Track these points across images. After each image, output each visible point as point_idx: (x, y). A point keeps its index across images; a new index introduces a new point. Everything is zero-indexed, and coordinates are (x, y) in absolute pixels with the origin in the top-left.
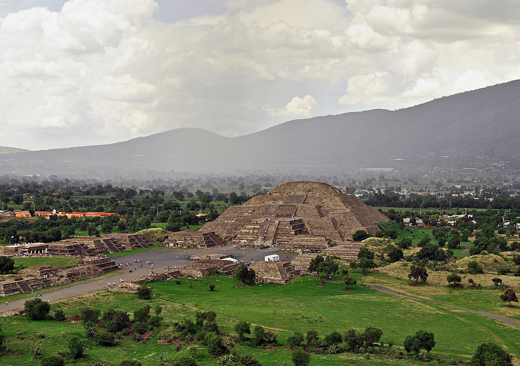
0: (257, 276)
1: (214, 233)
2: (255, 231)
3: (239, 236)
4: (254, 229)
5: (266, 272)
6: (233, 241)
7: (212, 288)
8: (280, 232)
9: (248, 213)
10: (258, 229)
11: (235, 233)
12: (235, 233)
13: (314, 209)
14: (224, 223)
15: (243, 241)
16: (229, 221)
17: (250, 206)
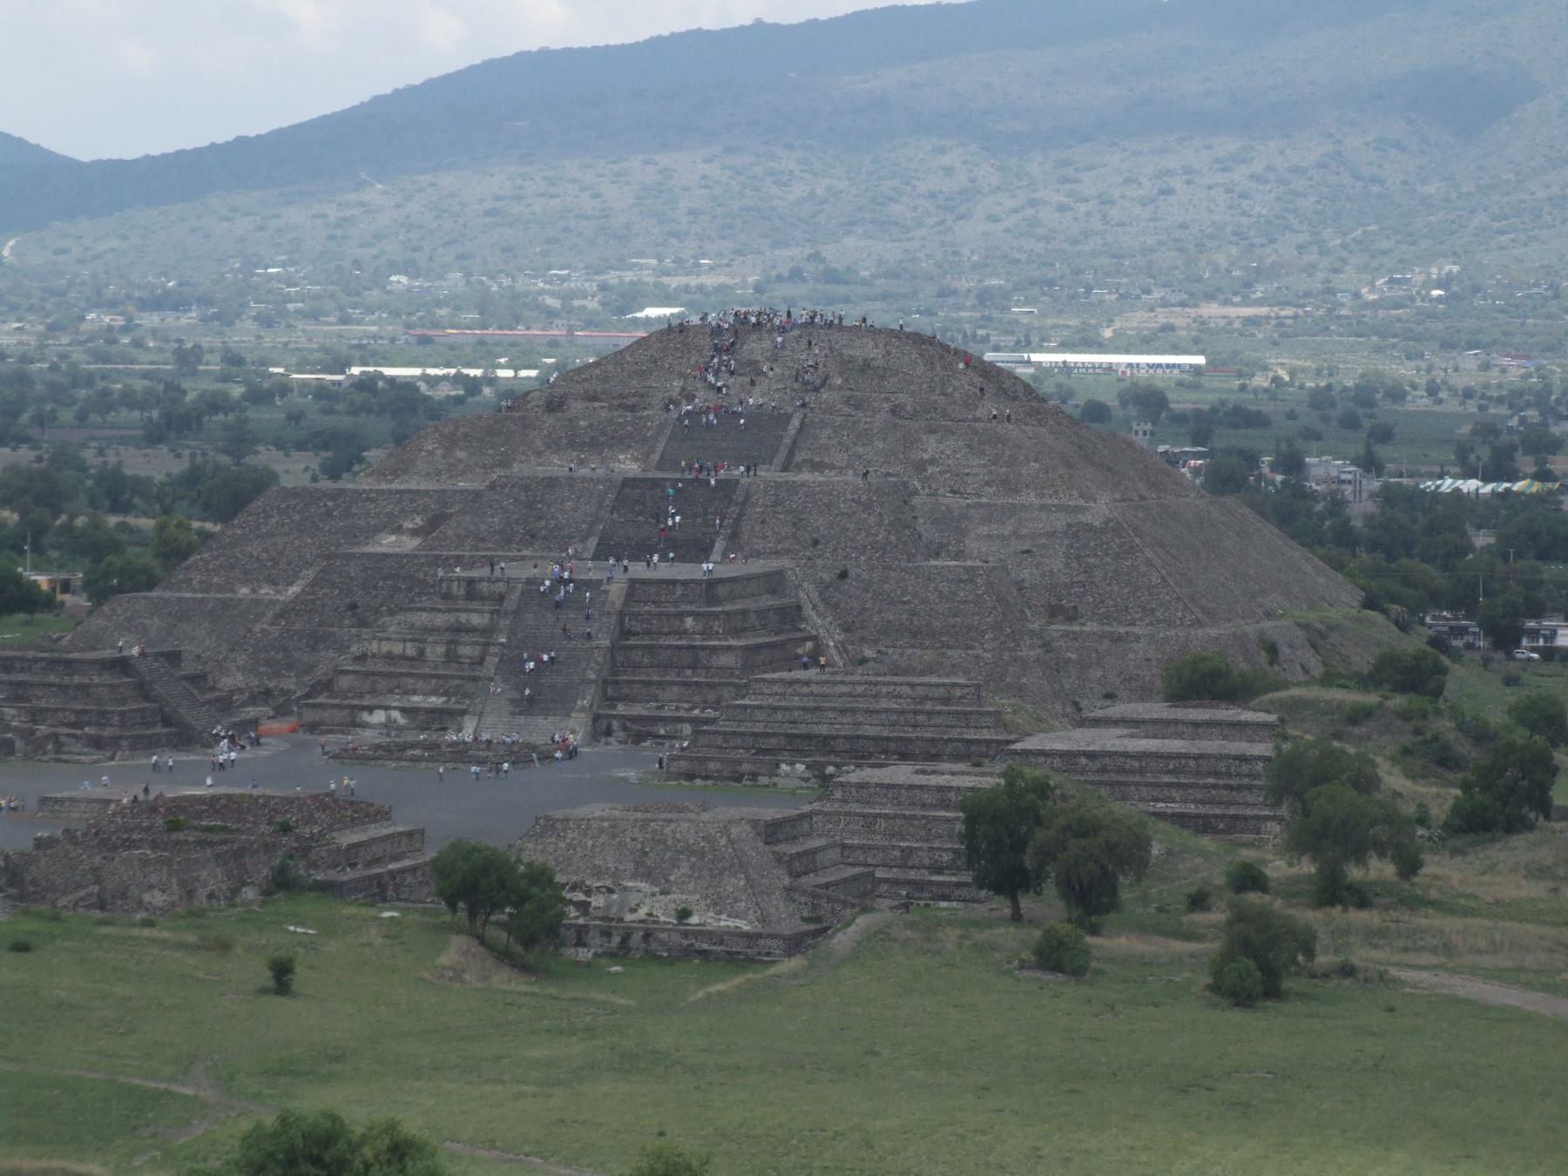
0: (583, 907)
1: (174, 657)
2: (465, 651)
3: (345, 682)
4: (459, 629)
5: (648, 875)
6: (310, 716)
7: (282, 976)
8: (636, 657)
9: (398, 530)
10: (488, 631)
11: (310, 669)
12: (310, 669)
13: (867, 507)
14: (226, 604)
15: (379, 717)
16: (266, 591)
17: (413, 486)
